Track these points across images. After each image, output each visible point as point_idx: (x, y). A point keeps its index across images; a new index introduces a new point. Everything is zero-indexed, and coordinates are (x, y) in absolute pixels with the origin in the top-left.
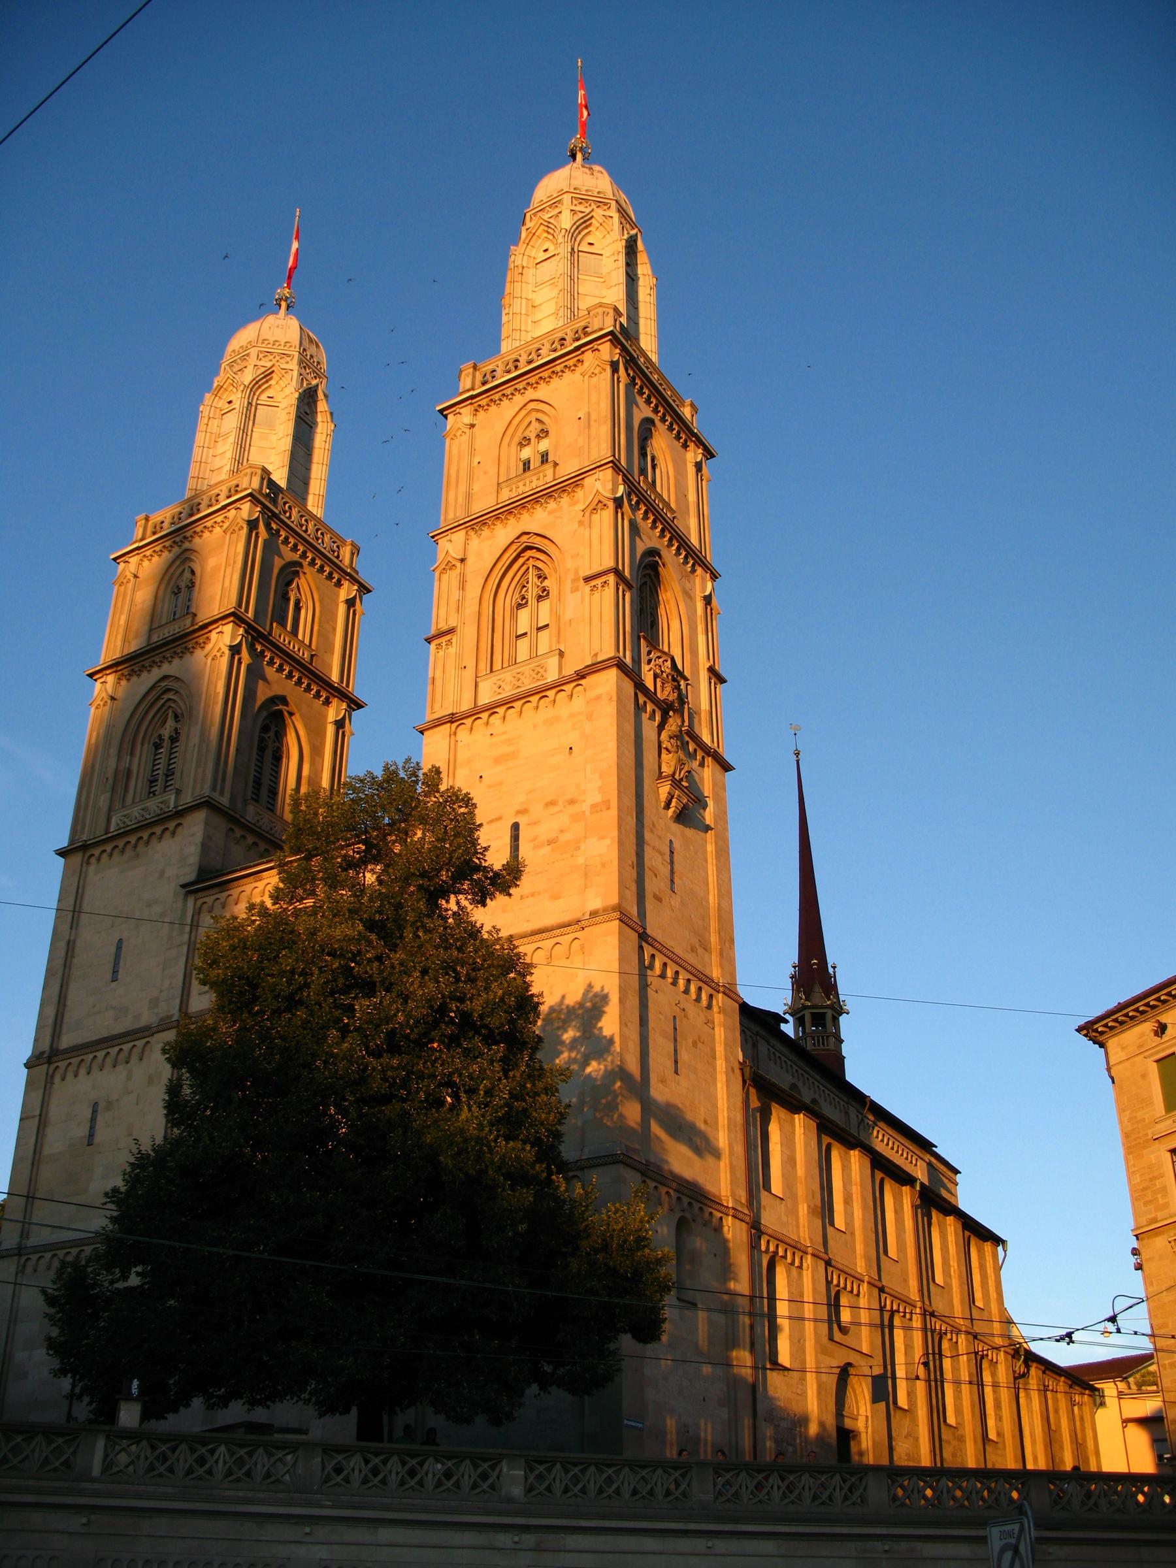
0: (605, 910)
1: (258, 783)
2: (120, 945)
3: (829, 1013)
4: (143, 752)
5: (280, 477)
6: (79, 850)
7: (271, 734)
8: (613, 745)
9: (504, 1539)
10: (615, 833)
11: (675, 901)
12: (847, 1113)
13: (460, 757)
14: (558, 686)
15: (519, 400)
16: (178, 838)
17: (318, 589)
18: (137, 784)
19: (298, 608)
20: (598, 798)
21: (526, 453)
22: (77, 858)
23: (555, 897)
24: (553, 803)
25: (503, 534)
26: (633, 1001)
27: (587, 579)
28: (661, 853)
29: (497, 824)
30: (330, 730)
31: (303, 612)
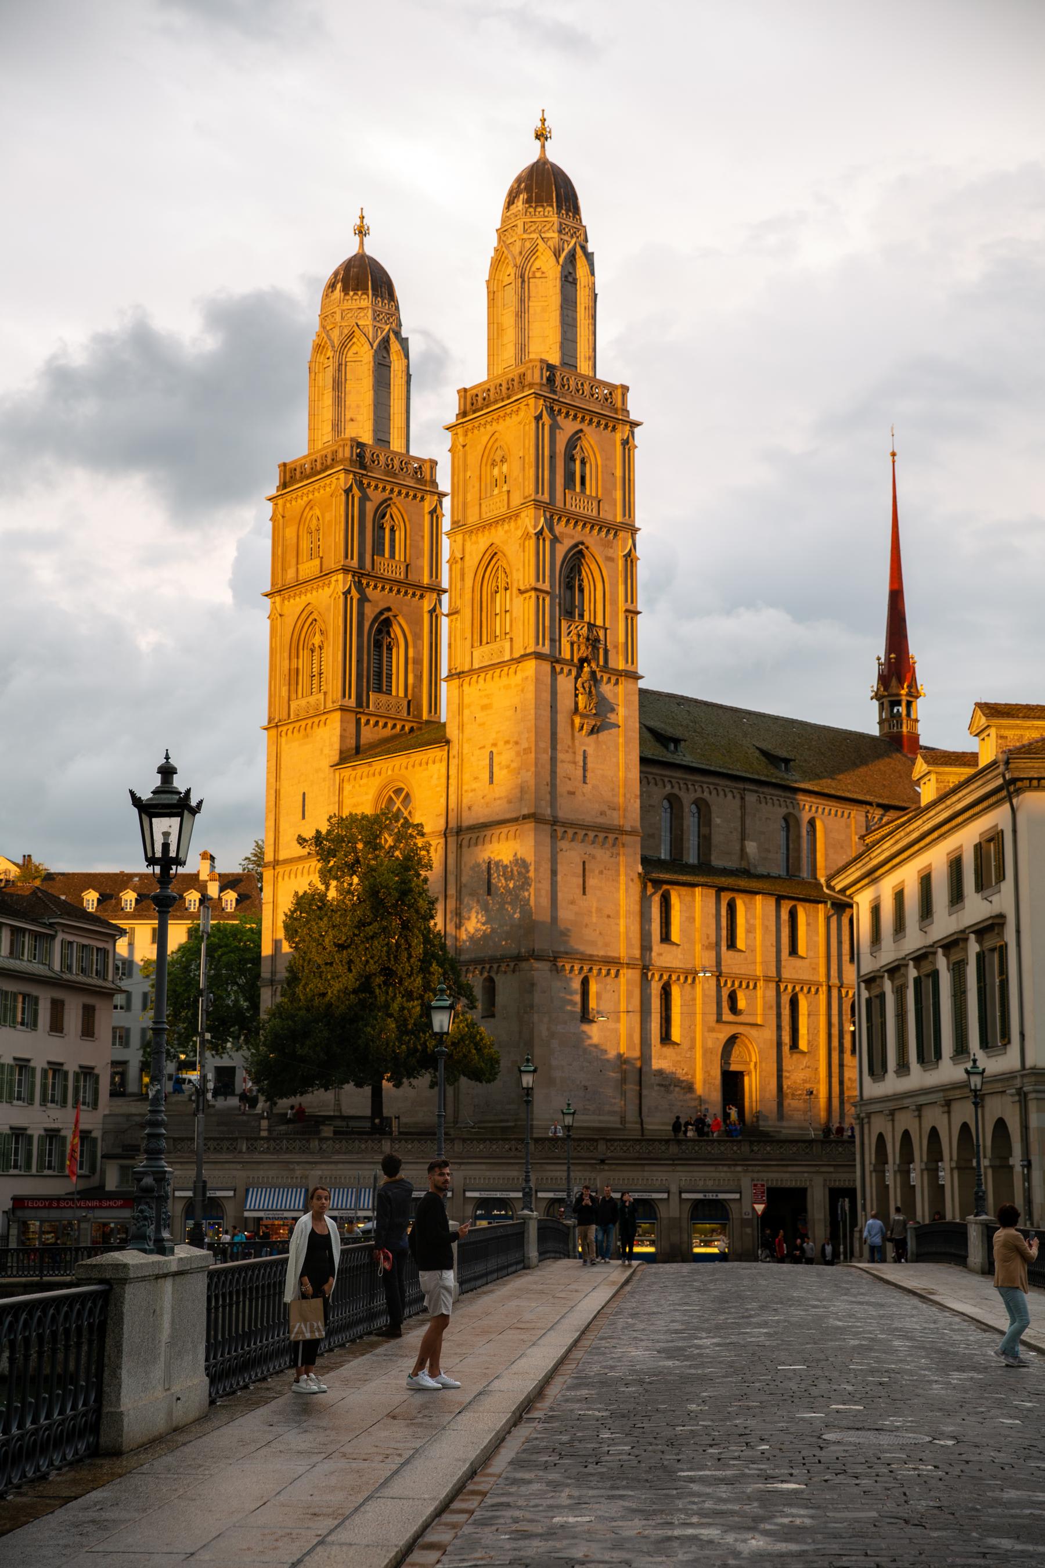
2: (304, 794)
4: (305, 654)
5: (367, 438)
8: (533, 712)
10: (533, 769)
13: (465, 702)
16: (327, 727)
17: (406, 512)
19: (392, 530)
20: (526, 746)
21: (496, 471)
22: (274, 731)
24: (507, 742)
26: (546, 867)
28: (575, 763)
29: (483, 750)
30: (426, 617)
31: (397, 533)
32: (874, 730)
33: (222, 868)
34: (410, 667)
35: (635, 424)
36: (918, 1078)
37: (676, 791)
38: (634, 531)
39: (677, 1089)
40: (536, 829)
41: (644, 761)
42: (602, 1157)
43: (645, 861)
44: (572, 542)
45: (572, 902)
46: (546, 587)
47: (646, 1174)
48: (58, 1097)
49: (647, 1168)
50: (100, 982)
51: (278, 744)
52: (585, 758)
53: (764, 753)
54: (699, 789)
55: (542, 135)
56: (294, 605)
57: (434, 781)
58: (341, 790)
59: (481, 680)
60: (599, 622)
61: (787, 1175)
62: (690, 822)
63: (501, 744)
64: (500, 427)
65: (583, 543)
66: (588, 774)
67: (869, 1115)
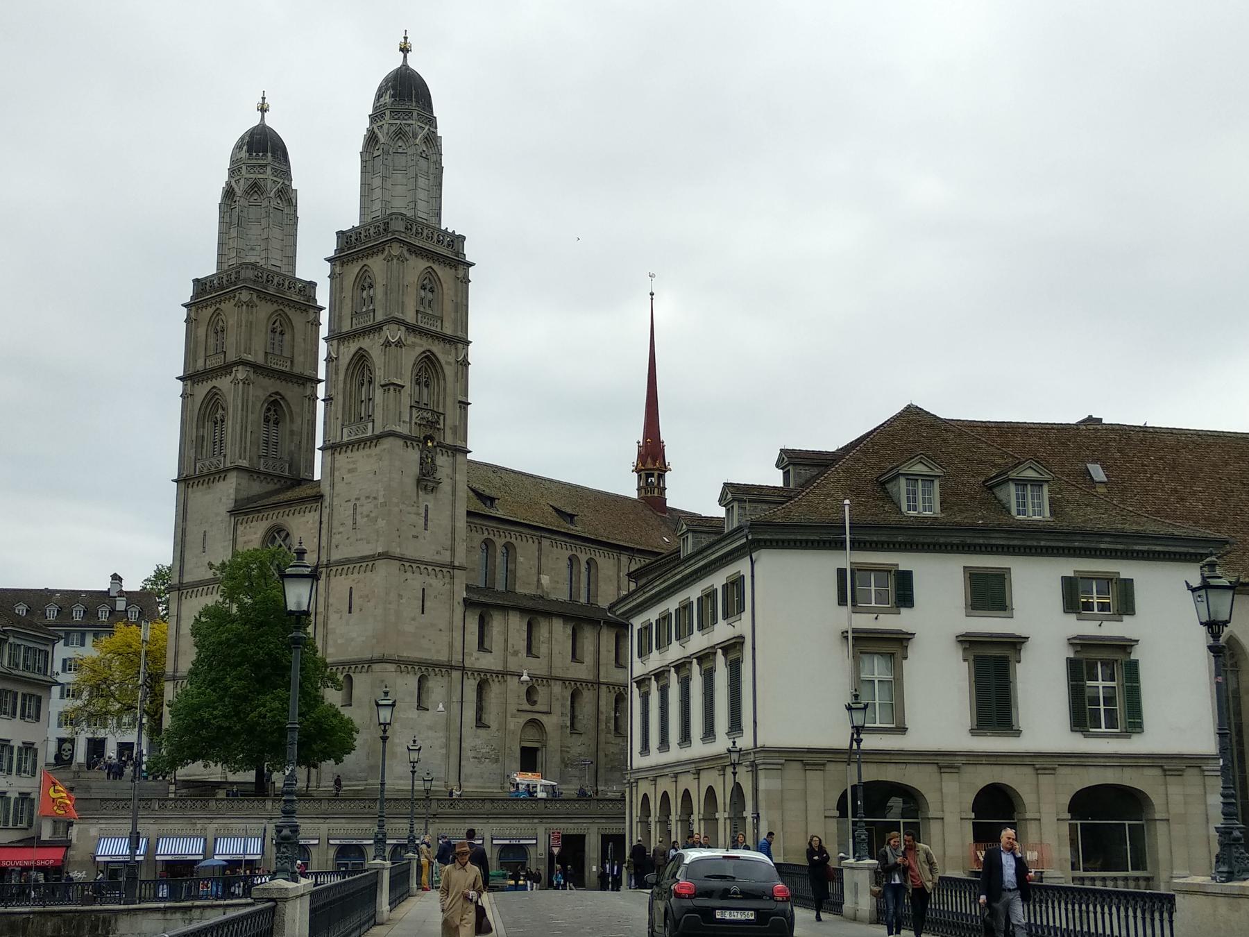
1: (267, 442)
4: (209, 425)
6: (184, 481)
14: (370, 440)
15: (361, 263)
18: (207, 445)
19: (282, 333)
22: (183, 485)
23: (368, 543)
24: (368, 497)
25: (353, 347)
28: (418, 514)
32: (634, 495)
33: (127, 587)
35: (471, 265)
36: (675, 753)
37: (491, 536)
38: (467, 343)
41: (469, 514)
43: (468, 588)
44: (422, 350)
45: (414, 619)
48: (29, 769)
50: (42, 677)
51: (186, 493)
52: (427, 511)
53: (557, 510)
55: (405, 50)
56: (202, 390)
57: (310, 525)
58: (235, 530)
62: (500, 559)
63: (363, 498)
64: (369, 262)
67: (637, 781)
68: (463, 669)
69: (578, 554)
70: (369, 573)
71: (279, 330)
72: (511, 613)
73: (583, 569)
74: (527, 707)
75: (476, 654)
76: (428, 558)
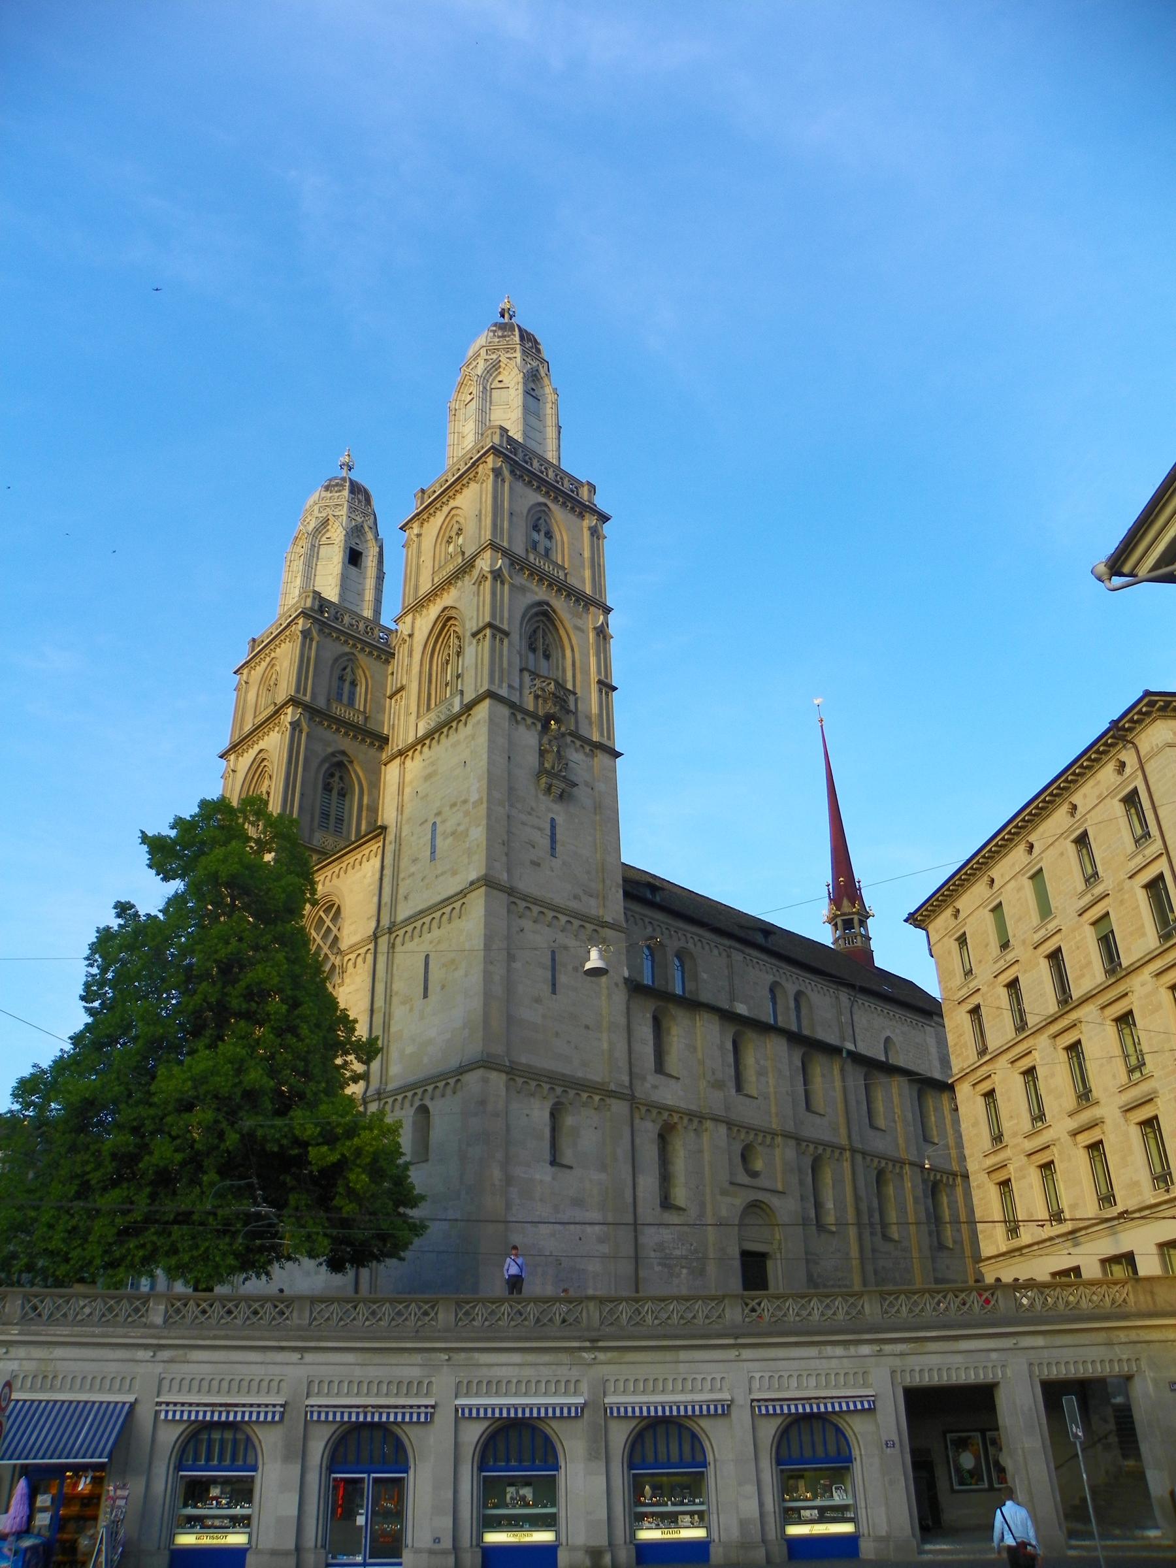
0: (478, 880)
3: (856, 918)
7: (336, 779)
8: (485, 756)
9: (141, 1354)
10: (484, 822)
11: (557, 863)
12: (837, 998)
14: (457, 718)
15: (446, 509)
21: (451, 549)
23: (455, 873)
24: (453, 805)
25: (434, 611)
27: (474, 635)
28: (539, 829)
34: (364, 814)
35: (604, 518)
39: (685, 1271)
40: (487, 895)
42: (594, 1334)
45: (538, 1000)
46: (505, 627)
47: (682, 1368)
49: (683, 1355)
54: (683, 938)
59: (426, 749)
60: (570, 686)
61: (959, 1358)
65: (548, 604)
66: (559, 847)
68: (631, 1099)
69: (784, 983)
70: (456, 923)
71: (349, 679)
72: (706, 1016)
73: (792, 1004)
74: (744, 1179)
75: (652, 1079)
76: (559, 899)
